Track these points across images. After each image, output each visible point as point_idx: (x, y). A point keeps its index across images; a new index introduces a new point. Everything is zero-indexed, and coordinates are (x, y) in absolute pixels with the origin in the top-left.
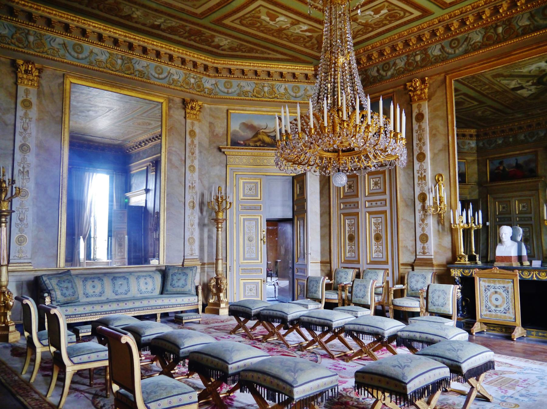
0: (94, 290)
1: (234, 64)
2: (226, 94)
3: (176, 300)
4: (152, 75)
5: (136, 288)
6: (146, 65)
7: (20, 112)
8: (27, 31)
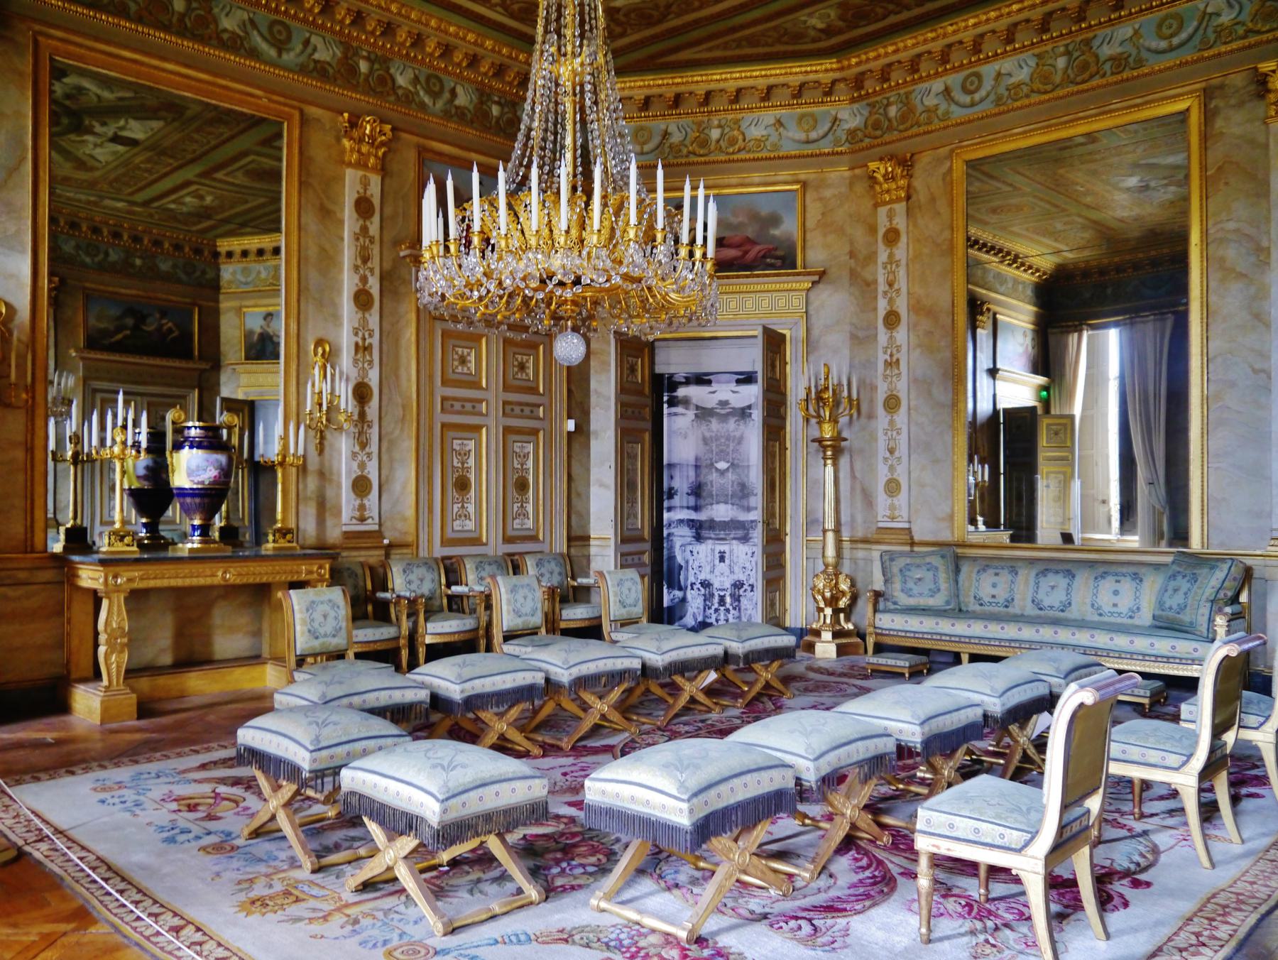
0: (994, 592)
3: (1132, 642)
4: (1149, 50)
5: (1088, 601)
6: (1130, 32)
7: (883, 256)
8: (885, 102)
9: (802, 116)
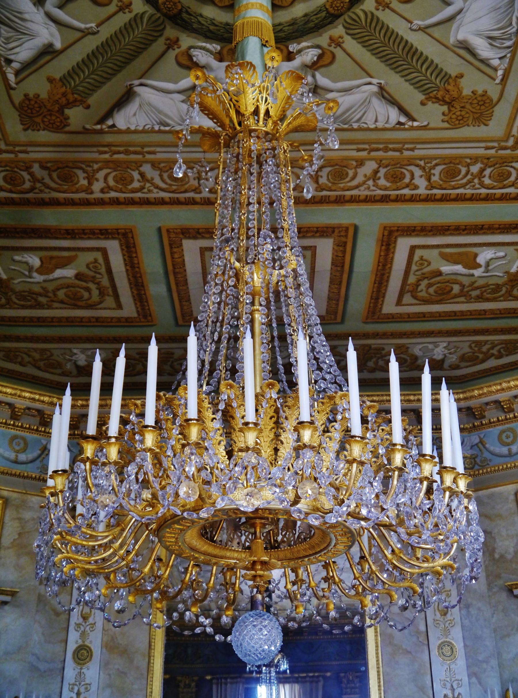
1: (503, 389)
2: (508, 459)
9: (14, 438)
